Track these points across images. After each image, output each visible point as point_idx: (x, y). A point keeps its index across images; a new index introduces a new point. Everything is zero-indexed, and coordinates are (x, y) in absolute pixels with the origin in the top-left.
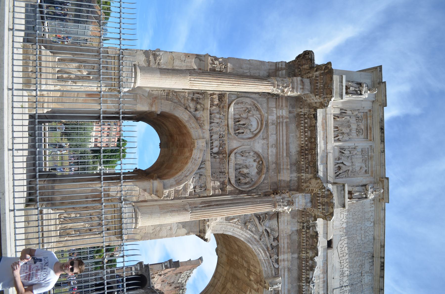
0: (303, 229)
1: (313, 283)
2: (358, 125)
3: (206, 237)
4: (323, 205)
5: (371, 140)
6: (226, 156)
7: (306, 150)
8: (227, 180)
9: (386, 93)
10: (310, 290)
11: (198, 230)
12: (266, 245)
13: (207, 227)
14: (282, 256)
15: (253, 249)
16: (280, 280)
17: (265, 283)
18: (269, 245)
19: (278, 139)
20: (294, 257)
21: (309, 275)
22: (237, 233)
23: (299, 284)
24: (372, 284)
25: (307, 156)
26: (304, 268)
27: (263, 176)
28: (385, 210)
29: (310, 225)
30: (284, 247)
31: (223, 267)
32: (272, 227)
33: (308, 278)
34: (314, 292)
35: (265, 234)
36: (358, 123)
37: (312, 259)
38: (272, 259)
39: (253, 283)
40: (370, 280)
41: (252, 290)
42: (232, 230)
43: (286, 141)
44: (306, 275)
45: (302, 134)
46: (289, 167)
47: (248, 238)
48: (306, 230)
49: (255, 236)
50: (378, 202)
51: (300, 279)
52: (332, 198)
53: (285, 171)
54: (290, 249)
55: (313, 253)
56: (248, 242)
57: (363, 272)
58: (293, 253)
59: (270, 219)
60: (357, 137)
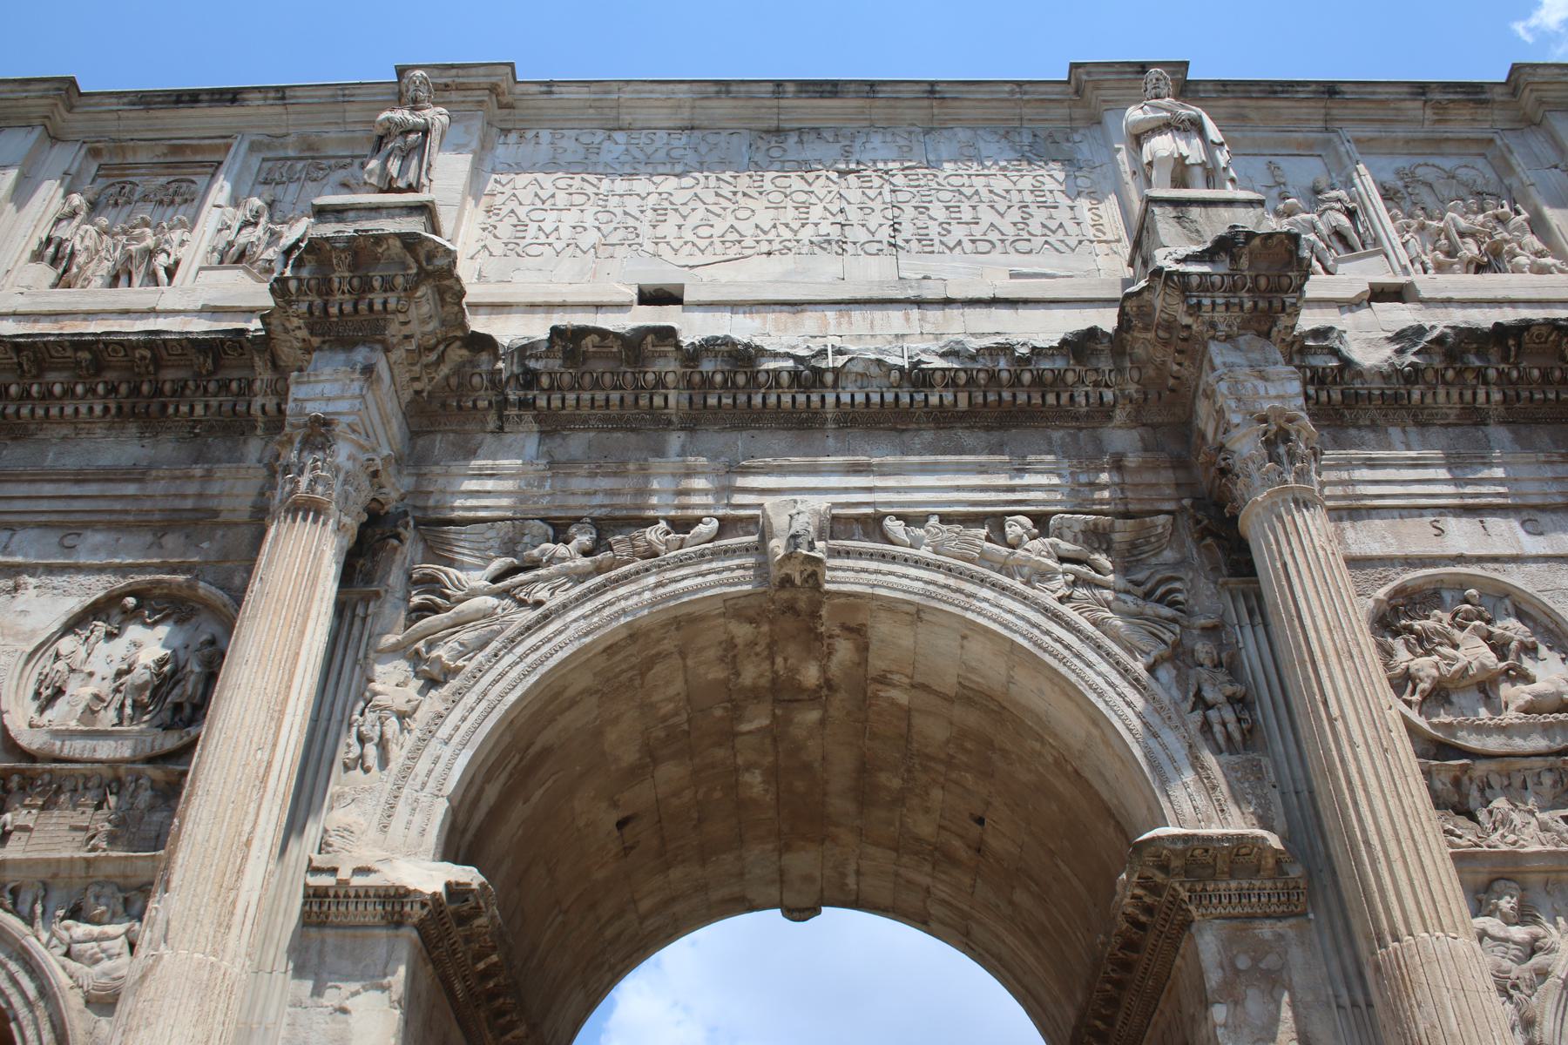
1: (822, 353)
2: (145, 198)
4: (367, 287)
5: (228, 147)
6: (21, 772)
7: (135, 391)
8: (153, 772)
9: (15, 80)
11: (383, 932)
12: (580, 577)
19: (43, 518)
21: (777, 372)
22: (465, 727)
23: (831, 425)
24: (910, 133)
25: (167, 387)
26: (742, 398)
27: (203, 588)
28: (550, 84)
29: (516, 369)
30: (611, 493)
33: (795, 375)
36: (136, 197)
37: (693, 356)
40: (889, 139)
41: (872, 672)
43: (62, 485)
45: (54, 411)
46: (198, 471)
48: (543, 390)
50: (516, 111)
52: (327, 239)
53: (215, 488)
54: (624, 463)
55: (664, 355)
57: (842, 166)
60: (196, 203)
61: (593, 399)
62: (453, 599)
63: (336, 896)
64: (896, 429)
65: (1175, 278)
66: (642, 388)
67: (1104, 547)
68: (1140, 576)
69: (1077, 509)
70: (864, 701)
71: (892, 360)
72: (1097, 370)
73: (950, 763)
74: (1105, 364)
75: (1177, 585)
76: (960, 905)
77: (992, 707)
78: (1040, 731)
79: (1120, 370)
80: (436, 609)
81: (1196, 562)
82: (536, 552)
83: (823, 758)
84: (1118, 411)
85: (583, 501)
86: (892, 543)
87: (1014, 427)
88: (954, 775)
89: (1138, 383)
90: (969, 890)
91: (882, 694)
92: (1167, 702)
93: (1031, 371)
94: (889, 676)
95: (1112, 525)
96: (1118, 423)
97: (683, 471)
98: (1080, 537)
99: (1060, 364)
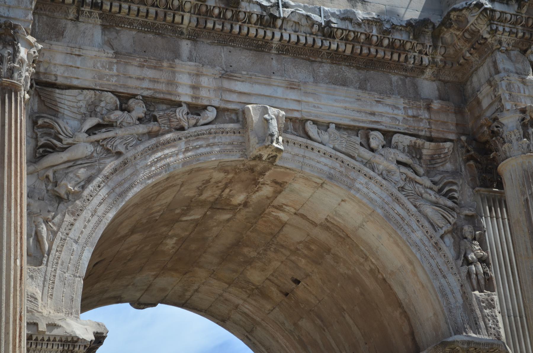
0: (101, 8)
1: (277, 5)
3: (90, 337)
10: (295, 19)
12: (140, 138)
13: (56, 332)
14: (180, 90)
15: (150, 182)
16: (254, 109)
17: (260, 157)
18: (142, 129)
20: (190, 52)
21: (251, 15)
22: (87, 232)
23: (274, 51)
26: (228, 27)
30: (154, 81)
31: (196, 291)
32: (83, 110)
33: (260, 18)
34: (305, 8)
35: (104, 136)
38: (186, 125)
39: (255, 197)
41: (275, 203)
42: (75, 246)
44: (250, 22)
47: (109, 194)
49: (107, 170)
51: (261, 46)
54: (160, 60)
56: (122, 195)
58: (177, 54)
59: (55, 113)
61: (139, 10)
62: (64, 142)
63: (36, 339)
64: (309, 60)
65: (488, 12)
66: (170, 9)
67: (418, 157)
68: (436, 179)
69: (406, 131)
70: (260, 215)
71: (315, 17)
72: (423, 44)
73: (295, 252)
74: (428, 42)
75: (455, 187)
76: (254, 317)
77: (341, 234)
78: (368, 254)
79: (435, 47)
80: (53, 149)
81: (464, 173)
82: (113, 117)
83: (216, 236)
84: (428, 70)
85: (137, 83)
86: (310, 138)
87: (373, 69)
88: (293, 258)
89: (442, 56)
90: (267, 312)
91: (273, 213)
92: (451, 259)
93: (389, 38)
94: (284, 207)
95: (423, 144)
96: (427, 77)
97: (195, 72)
98: (406, 149)
99: (404, 37)
